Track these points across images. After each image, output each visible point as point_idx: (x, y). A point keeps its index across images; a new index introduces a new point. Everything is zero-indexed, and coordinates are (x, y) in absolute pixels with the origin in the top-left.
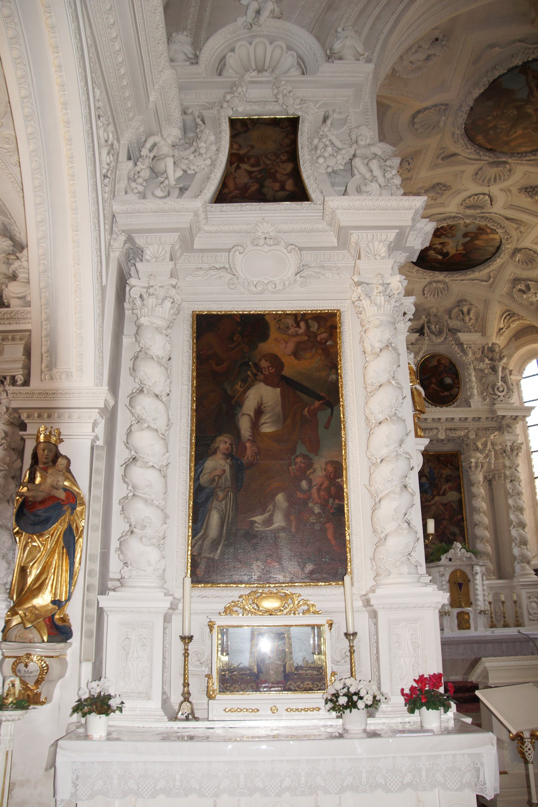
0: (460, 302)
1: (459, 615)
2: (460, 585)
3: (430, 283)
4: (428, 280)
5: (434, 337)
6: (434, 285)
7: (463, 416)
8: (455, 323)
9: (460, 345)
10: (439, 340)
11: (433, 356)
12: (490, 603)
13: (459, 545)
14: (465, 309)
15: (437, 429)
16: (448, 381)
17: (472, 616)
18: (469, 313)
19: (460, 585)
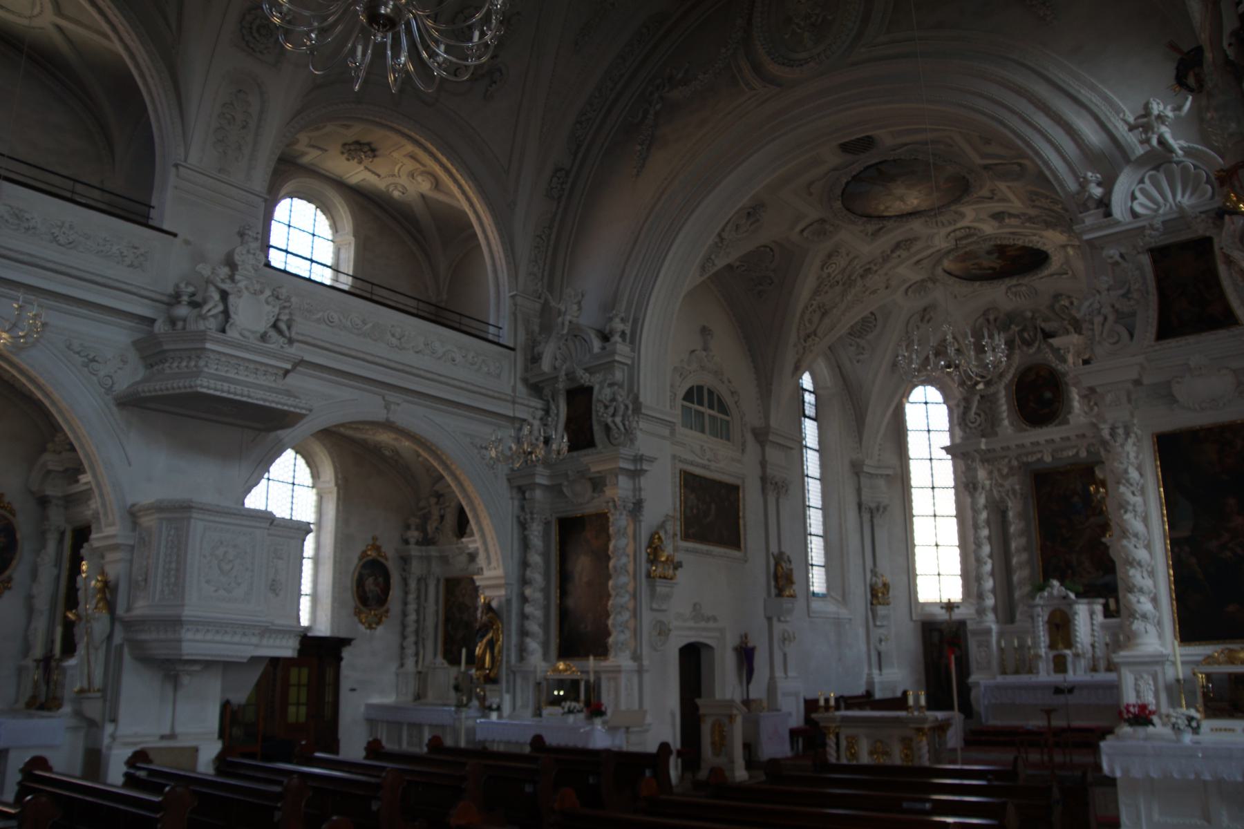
0: (1057, 297)
1: (1055, 657)
2: (1057, 626)
3: (1009, 288)
4: (1003, 287)
5: (1025, 348)
6: (1014, 289)
7: (1064, 435)
8: (1047, 327)
9: (1056, 351)
10: (1032, 351)
11: (1029, 369)
12: (1107, 645)
13: (1056, 583)
14: (1067, 303)
15: (1041, 452)
16: (1048, 395)
17: (1069, 659)
18: (1072, 303)
19: (1057, 626)
